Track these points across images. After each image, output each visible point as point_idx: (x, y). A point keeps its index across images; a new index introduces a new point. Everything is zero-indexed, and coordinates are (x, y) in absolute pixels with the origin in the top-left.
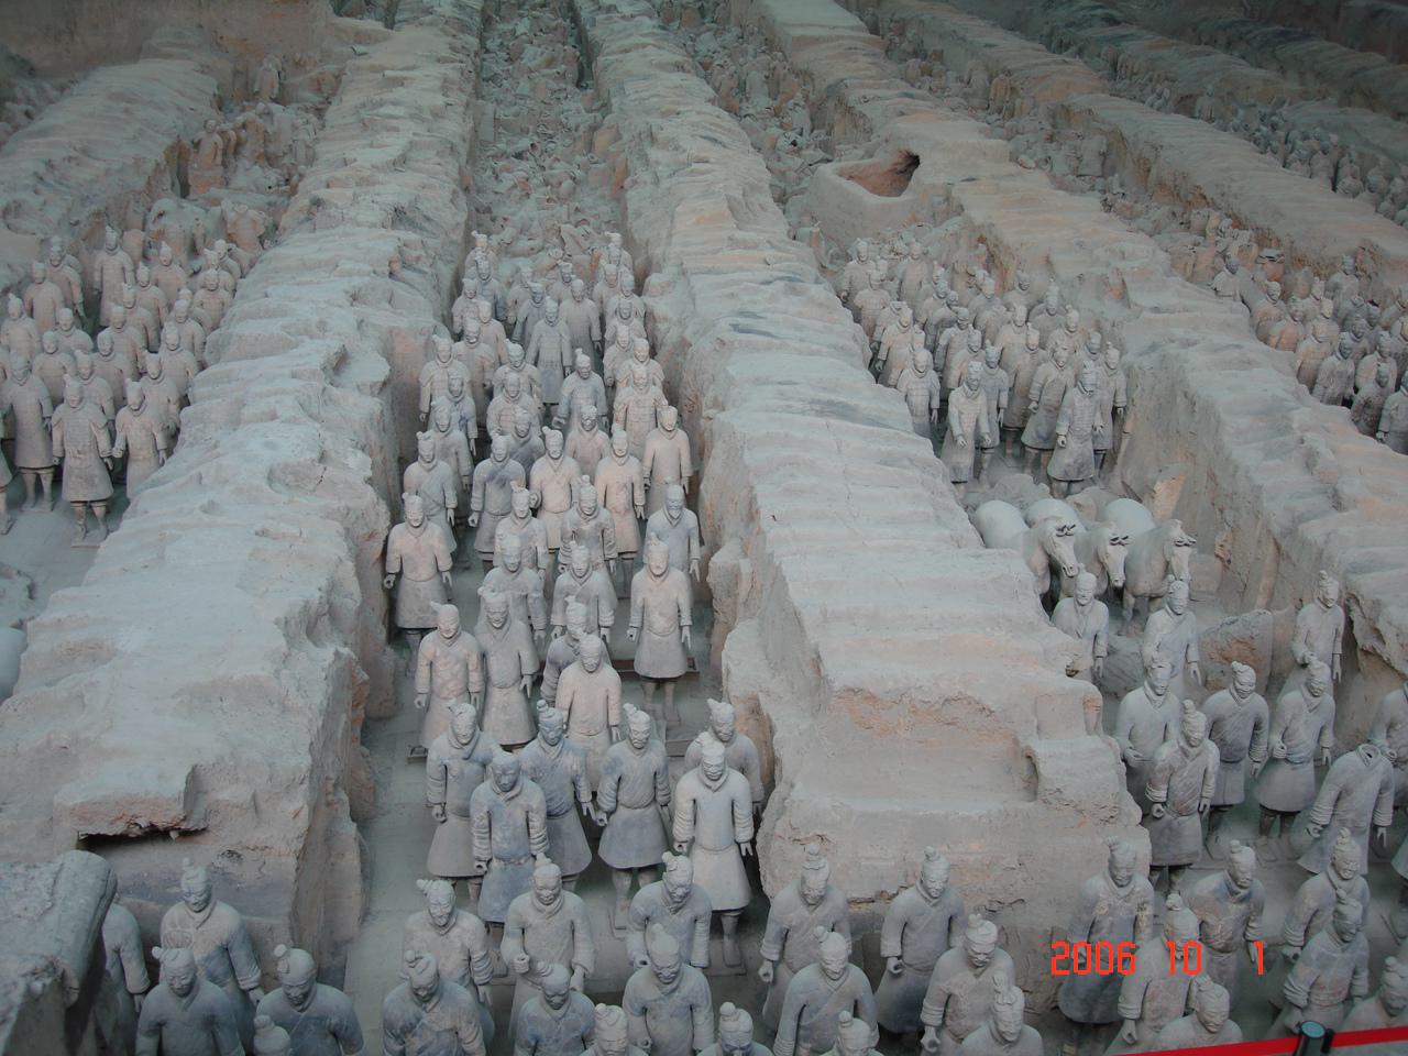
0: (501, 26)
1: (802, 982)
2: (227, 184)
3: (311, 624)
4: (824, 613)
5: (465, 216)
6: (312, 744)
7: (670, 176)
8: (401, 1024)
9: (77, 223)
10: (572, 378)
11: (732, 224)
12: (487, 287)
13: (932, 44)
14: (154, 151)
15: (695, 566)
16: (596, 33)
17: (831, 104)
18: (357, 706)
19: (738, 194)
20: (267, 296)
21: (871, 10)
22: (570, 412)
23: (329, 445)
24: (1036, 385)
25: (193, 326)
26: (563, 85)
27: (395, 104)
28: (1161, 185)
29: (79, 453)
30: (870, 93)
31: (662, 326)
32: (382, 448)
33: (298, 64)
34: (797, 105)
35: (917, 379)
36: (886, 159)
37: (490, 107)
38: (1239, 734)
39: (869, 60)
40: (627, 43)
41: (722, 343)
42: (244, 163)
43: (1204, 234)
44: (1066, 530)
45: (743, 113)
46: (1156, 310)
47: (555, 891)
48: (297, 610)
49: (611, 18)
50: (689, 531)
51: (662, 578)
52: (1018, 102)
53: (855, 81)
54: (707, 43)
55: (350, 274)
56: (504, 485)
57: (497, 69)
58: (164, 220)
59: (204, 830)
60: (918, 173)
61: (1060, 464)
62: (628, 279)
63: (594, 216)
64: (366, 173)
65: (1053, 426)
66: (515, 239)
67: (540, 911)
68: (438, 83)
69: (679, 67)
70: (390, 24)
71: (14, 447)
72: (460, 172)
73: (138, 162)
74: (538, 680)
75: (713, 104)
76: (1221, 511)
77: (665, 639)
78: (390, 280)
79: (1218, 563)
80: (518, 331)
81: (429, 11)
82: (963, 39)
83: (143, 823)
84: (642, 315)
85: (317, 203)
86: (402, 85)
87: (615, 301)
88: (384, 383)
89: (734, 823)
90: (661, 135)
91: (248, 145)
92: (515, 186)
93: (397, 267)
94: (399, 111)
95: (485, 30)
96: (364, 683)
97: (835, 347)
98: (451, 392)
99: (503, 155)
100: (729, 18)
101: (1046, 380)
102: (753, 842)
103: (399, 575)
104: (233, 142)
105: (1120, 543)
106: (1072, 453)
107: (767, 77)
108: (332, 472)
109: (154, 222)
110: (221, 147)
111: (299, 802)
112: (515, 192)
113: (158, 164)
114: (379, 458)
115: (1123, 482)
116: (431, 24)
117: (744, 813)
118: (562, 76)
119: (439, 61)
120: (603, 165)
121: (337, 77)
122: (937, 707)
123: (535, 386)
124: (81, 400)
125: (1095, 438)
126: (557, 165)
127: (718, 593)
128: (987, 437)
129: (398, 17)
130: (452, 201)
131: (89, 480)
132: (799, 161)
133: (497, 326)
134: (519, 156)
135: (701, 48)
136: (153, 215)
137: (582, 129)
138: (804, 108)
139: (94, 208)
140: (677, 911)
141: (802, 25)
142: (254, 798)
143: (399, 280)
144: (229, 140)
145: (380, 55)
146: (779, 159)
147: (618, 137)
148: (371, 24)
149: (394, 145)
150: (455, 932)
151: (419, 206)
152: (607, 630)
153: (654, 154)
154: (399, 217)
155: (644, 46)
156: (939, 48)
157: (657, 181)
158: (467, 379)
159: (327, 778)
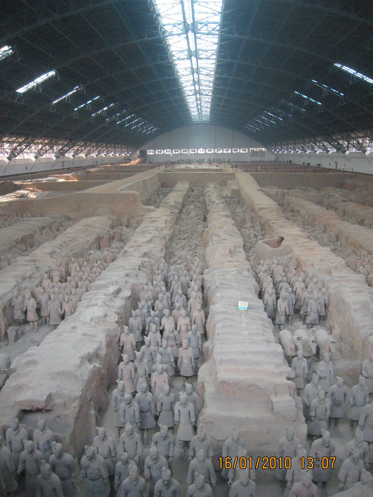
0: (188, 207)
1: (193, 462)
2: (110, 247)
3: (90, 358)
4: (221, 360)
5: (164, 254)
6: (82, 390)
7: (217, 244)
8: (85, 466)
9: (69, 256)
11: (230, 256)
13: (296, 208)
14: (92, 239)
15: (200, 346)
16: (209, 208)
18: (103, 380)
19: (233, 248)
21: (281, 200)
23: (108, 313)
25: (87, 282)
26: (199, 221)
27: (152, 227)
28: (351, 244)
30: (275, 221)
31: (206, 283)
32: (125, 314)
33: (133, 217)
36: (276, 238)
37: (178, 227)
38: (339, 397)
39: (278, 213)
40: (215, 210)
41: (217, 287)
42: (115, 241)
43: (360, 256)
45: (244, 227)
46: (339, 277)
47: (131, 433)
48: (86, 354)
50: (198, 337)
52: (316, 222)
54: (239, 210)
55: (128, 269)
57: (184, 217)
58: (91, 256)
59: (51, 410)
60: (283, 242)
61: (308, 320)
62: (198, 270)
65: (307, 309)
66: (177, 260)
67: (128, 438)
69: (227, 216)
70: (158, 208)
71: (40, 311)
72: (166, 243)
73: (87, 241)
74: (150, 375)
75: (234, 225)
76: (351, 333)
78: (138, 271)
79: (350, 347)
80: (169, 283)
81: (167, 203)
82: (304, 207)
83: (35, 407)
84: (201, 279)
85: (126, 252)
87: (195, 276)
88: (130, 297)
89: (190, 417)
90: (216, 233)
92: (181, 247)
93: (141, 267)
94: (153, 228)
95: (183, 208)
96: (104, 374)
97: (247, 288)
98: (145, 299)
99: (180, 239)
101: (305, 297)
102: (196, 422)
103: (123, 347)
106: (312, 317)
108: (107, 319)
111: (76, 404)
113: (93, 242)
114: (124, 316)
115: (329, 324)
116: (166, 207)
117: (192, 414)
118: (199, 219)
121: (142, 220)
122: (247, 387)
124: (54, 300)
125: (318, 312)
127: (205, 354)
128: (288, 312)
129: (161, 205)
130: (161, 251)
132: (255, 239)
133: (162, 283)
135: (237, 211)
136: (88, 254)
137: (200, 232)
138: (259, 226)
139: (73, 252)
140: (164, 440)
142: (65, 403)
143: (142, 271)
145: (153, 215)
146: (250, 239)
147: (208, 234)
148: (152, 207)
149: (149, 237)
150: (105, 442)
154: (145, 255)
155: (219, 211)
156: (298, 209)
157: (213, 246)
158: (151, 296)
159: (87, 399)
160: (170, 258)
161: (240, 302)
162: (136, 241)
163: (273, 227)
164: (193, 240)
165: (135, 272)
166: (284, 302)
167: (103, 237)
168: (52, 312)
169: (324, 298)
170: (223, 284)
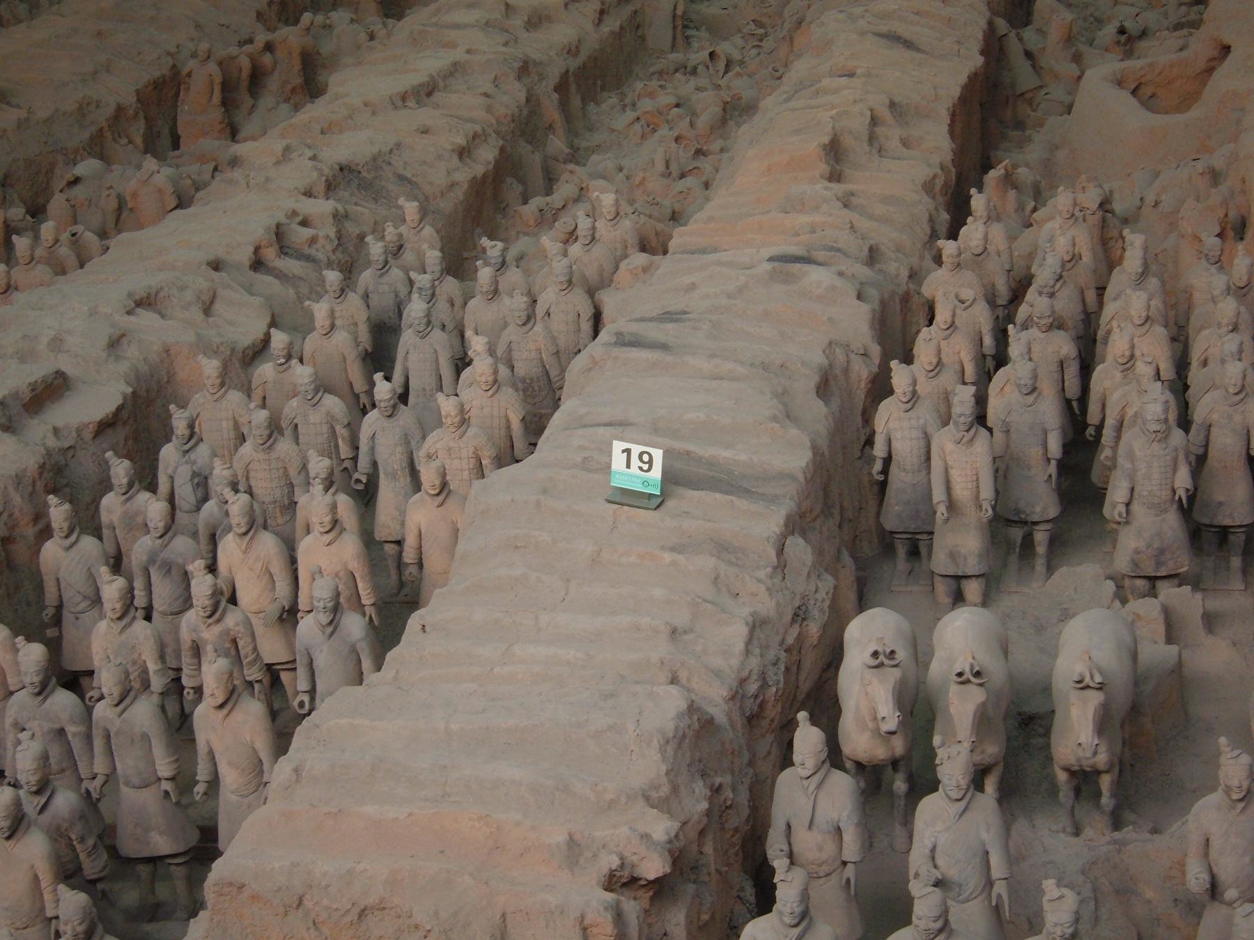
5: (479, 170)
10: (373, 415)
11: (823, 168)
12: (385, 279)
19: (858, 123)
22: (375, 464)
24: (1110, 422)
35: (902, 414)
42: (267, 100)
44: (882, 658)
51: (225, 711)
56: (169, 571)
77: (246, 801)
88: (104, 426)
91: (276, 72)
93: (270, 254)
97: (765, 367)
104: (245, 74)
105: (968, 681)
109: (61, 191)
110: (218, 79)
112: (637, 127)
113: (120, 109)
114: (30, 531)
123: (338, 428)
137: (787, 25)
143: (271, 271)
144: (241, 70)
151: (394, 159)
152: (169, 782)
160: (550, 182)
161: (618, 446)
164: (739, 75)
165: (202, 281)
166: (972, 440)
167: (189, 75)
169: (1238, 418)
170: (635, 342)
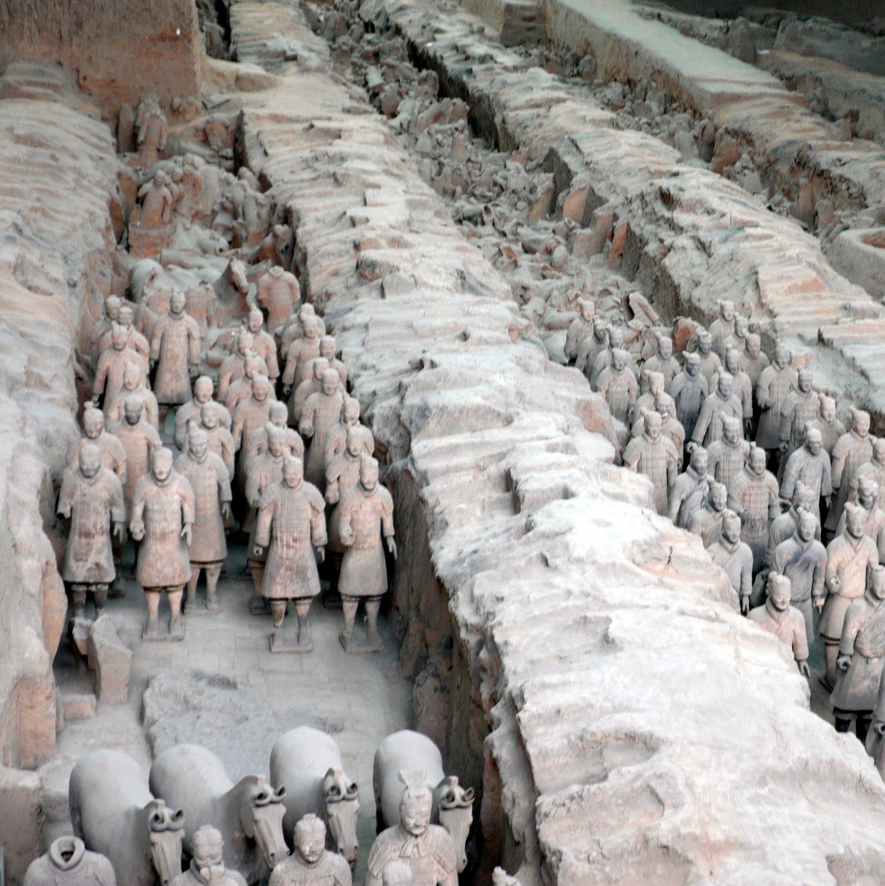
7: (725, 240)
16: (479, 84)
17: (784, 168)
20: (433, 365)
27: (363, 157)
29: (295, 540)
30: (845, 155)
34: (745, 168)
40: (538, 95)
49: (490, 69)
53: (820, 143)
63: (612, 285)
64: (396, 233)
68: (382, 138)
69: (615, 125)
86: (339, 137)
90: (685, 196)
94: (370, 166)
100: (595, 71)
107: (696, 138)
119: (348, 111)
120: (588, 231)
126: (520, 230)
131: (301, 573)
134: (469, 219)
137: (540, 190)
138: (753, 171)
141: (715, 81)
147: (594, 200)
153: (682, 218)
157: (703, 247)
162: (353, 223)
163: (843, 179)
164: (519, 224)
168: (283, 536)
